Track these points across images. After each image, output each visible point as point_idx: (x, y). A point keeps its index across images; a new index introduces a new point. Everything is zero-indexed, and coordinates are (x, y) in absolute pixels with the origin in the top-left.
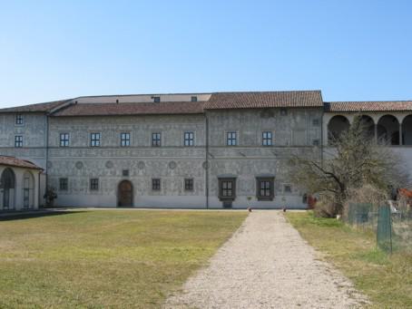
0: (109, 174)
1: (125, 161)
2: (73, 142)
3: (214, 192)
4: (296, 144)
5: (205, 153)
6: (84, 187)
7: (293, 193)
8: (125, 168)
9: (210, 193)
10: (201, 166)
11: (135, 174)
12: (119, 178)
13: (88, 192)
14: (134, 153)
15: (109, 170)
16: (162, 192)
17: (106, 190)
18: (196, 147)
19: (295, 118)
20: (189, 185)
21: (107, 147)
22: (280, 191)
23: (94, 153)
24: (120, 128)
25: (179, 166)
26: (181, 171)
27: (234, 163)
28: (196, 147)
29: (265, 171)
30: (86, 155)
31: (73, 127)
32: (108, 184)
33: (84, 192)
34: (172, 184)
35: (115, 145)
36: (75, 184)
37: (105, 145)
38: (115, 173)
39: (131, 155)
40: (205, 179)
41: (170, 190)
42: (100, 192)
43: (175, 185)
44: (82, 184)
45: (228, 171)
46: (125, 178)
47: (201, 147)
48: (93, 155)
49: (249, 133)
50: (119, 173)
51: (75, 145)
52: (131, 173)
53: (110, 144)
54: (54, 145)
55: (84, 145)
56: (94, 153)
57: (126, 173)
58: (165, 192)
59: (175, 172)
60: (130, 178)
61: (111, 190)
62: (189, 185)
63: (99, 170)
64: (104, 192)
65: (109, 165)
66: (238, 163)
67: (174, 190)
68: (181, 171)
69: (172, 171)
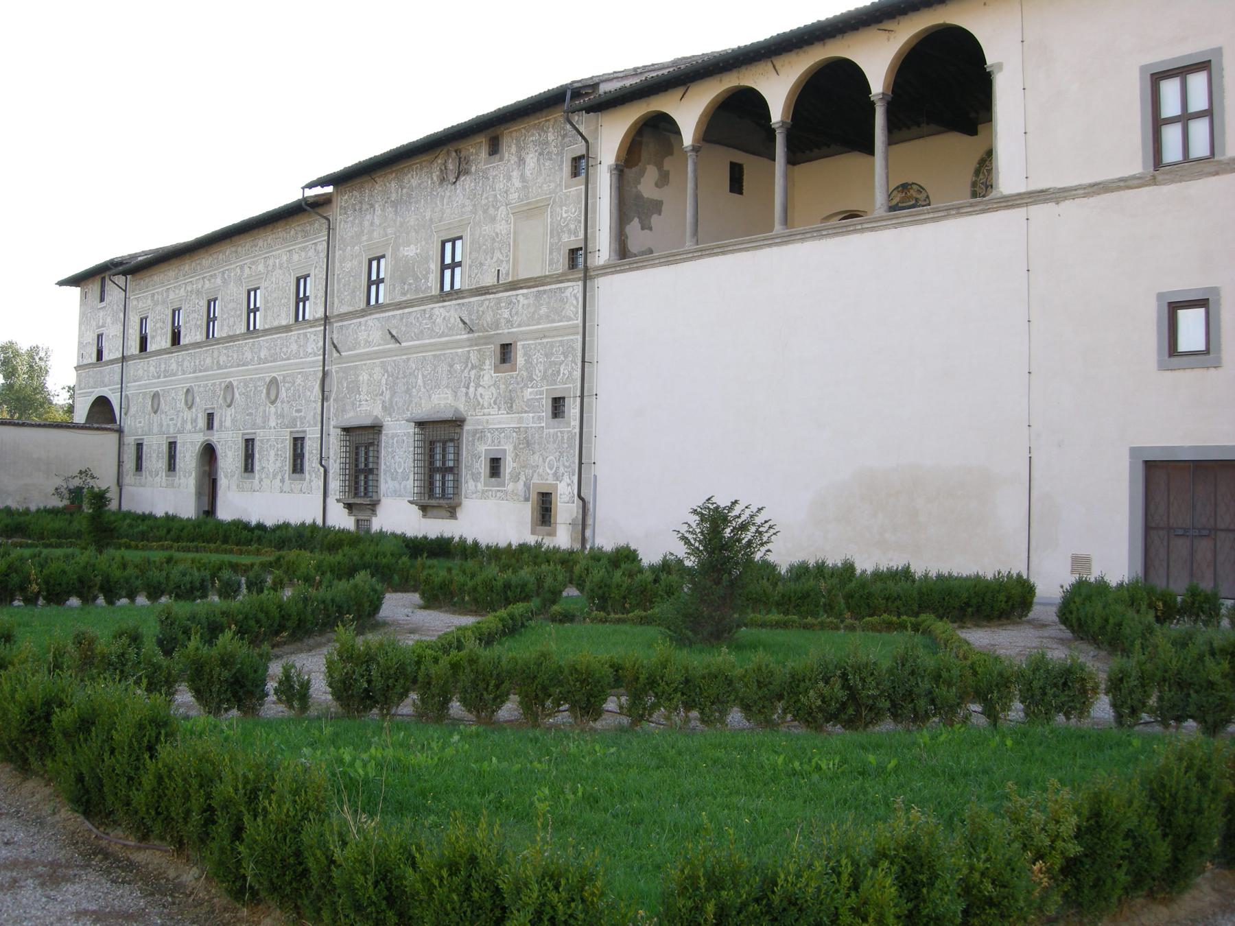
4: (523, 275)
7: (510, 487)
19: (521, 161)
22: (476, 478)
29: (439, 403)
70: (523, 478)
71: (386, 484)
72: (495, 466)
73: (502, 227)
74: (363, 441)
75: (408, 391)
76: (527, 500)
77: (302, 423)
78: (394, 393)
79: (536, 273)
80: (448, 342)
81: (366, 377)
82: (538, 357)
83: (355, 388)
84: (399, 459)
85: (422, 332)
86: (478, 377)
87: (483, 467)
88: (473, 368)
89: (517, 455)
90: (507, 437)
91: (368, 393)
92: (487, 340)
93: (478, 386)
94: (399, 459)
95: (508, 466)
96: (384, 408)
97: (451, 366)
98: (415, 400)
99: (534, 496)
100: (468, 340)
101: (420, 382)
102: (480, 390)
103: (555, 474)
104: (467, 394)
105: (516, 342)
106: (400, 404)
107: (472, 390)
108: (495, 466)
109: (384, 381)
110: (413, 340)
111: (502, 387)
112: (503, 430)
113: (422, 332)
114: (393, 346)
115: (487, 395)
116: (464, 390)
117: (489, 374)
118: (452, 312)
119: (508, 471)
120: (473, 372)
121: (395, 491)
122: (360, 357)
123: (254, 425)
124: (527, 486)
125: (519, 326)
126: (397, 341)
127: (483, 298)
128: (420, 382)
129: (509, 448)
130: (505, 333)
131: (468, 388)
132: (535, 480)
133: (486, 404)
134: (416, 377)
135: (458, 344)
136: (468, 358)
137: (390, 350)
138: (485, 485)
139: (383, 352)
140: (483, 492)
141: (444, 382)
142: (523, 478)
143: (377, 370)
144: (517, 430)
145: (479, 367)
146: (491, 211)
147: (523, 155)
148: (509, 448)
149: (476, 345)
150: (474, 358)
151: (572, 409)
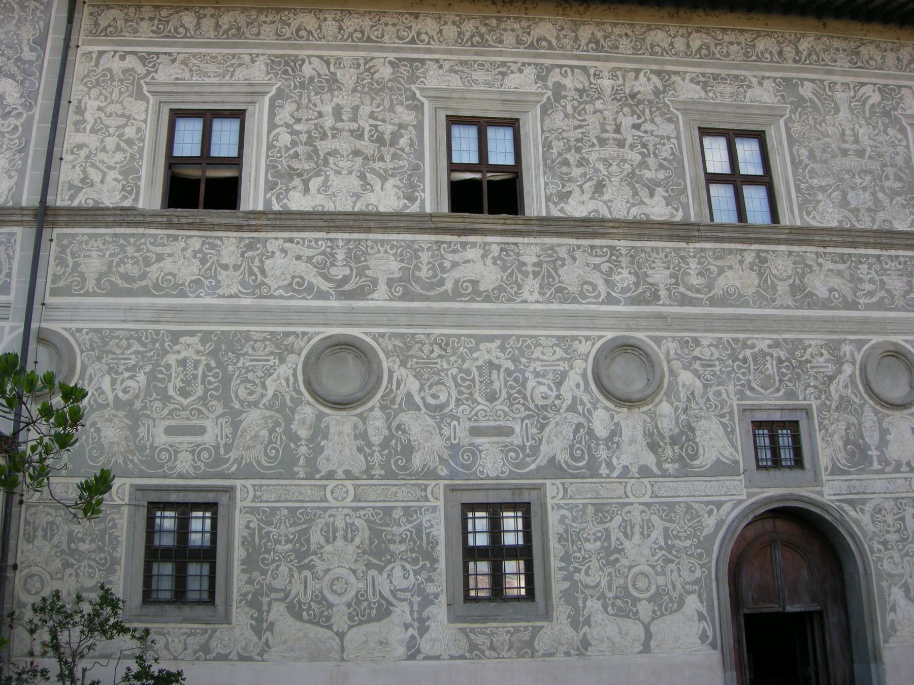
0: (634, 453)
1: (762, 342)
2: (282, 176)
6: (399, 577)
8: (771, 403)
11: (858, 455)
12: (734, 495)
13: (442, 630)
14: (819, 286)
15: (632, 424)
17: (623, 605)
21: (588, 227)
23: (490, 276)
24: (688, 91)
30: (405, 285)
31: (287, 66)
32: (638, 552)
33: (395, 630)
35: (658, 209)
36: (302, 554)
37: (578, 207)
38: (685, 437)
39: (803, 295)
42: (557, 629)
44: (378, 553)
46: (779, 488)
48: (475, 291)
50: (720, 441)
51: (298, 202)
52: (825, 446)
53: (618, 204)
54: (109, 195)
55: (386, 199)
56: (490, 276)
57: (779, 440)
60: (825, 489)
61: (665, 602)
63: (540, 416)
64: (605, 628)
65: (627, 375)
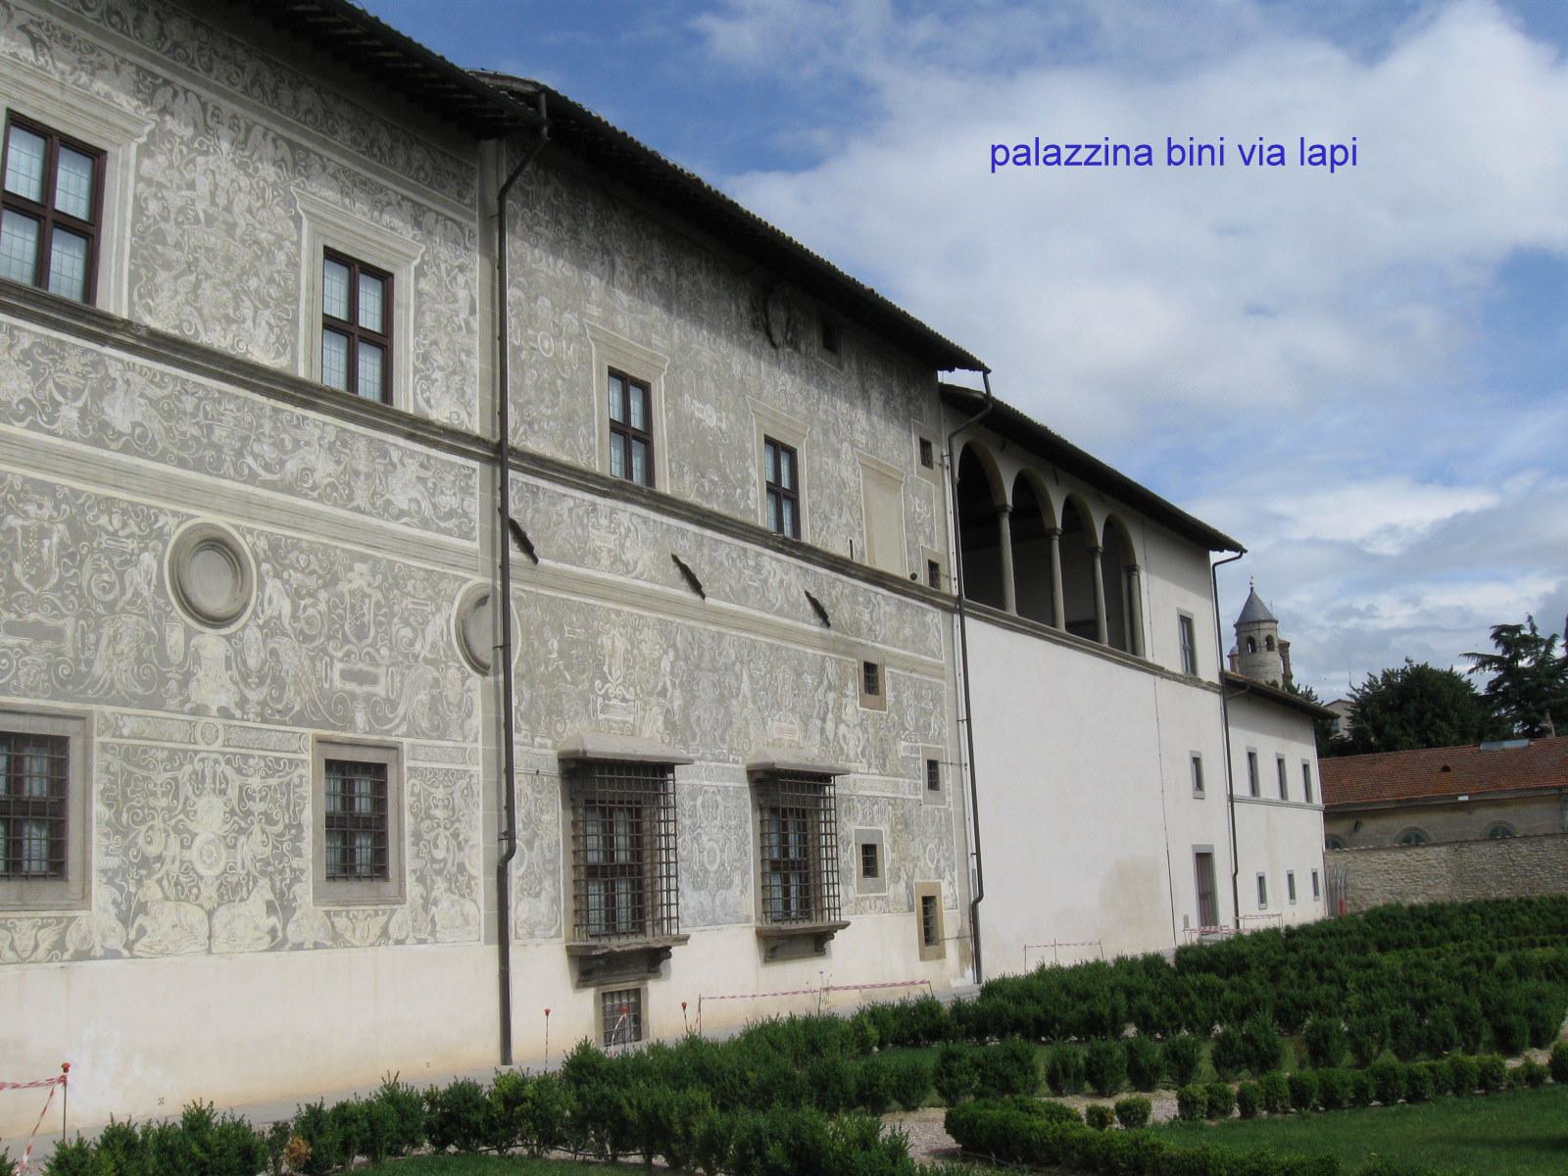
3: (543, 906)
5: (477, 506)
9: (518, 911)
10: (442, 623)
16: (99, 913)
18: (419, 429)
20: (359, 828)
25: (274, 598)
26: (292, 657)
27: (650, 642)
28: (419, 429)
34: (210, 816)
40: (479, 770)
41: (184, 889)
43: (240, 817)
45: (626, 730)
47: (452, 439)
49: (708, 416)
58: (130, 913)
59: (235, 660)
62: (359, 828)
66: (665, 631)
67: (230, 891)
68: (292, 657)
69: (211, 642)
70: (904, 876)
71: (688, 901)
72: (870, 855)
73: (847, 473)
74: (617, 799)
75: (721, 700)
76: (911, 909)
77: (376, 718)
78: (690, 700)
79: (882, 565)
80: (788, 629)
81: (621, 645)
82: (907, 696)
83: (587, 660)
84: (713, 843)
85: (744, 590)
86: (840, 707)
87: (851, 859)
88: (830, 688)
89: (895, 841)
90: (882, 812)
91: (626, 682)
92: (849, 649)
93: (839, 721)
94: (713, 843)
95: (887, 858)
96: (670, 725)
97: (799, 674)
98: (738, 723)
99: (919, 904)
100: (822, 637)
101: (745, 687)
102: (842, 729)
103: (937, 868)
104: (823, 731)
105: (883, 666)
106: (707, 725)
107: (830, 725)
108: (870, 855)
109: (666, 665)
110: (727, 599)
111: (871, 730)
112: (875, 800)
113: (744, 590)
114: (684, 593)
115: (853, 741)
116: (819, 723)
117: (853, 706)
118: (792, 576)
119: (887, 866)
120: (831, 696)
121: (702, 914)
122: (606, 591)
123: (75, 681)
124: (908, 887)
125: (884, 642)
126: (696, 586)
127: (834, 575)
128: (745, 687)
129: (884, 828)
130: (879, 648)
131: (824, 720)
132: (917, 879)
133: (852, 754)
134: (739, 678)
135: (805, 638)
136: (823, 669)
137: (678, 602)
138: (860, 890)
139: (647, 595)
140: (858, 902)
141: (787, 701)
142: (904, 876)
143: (649, 634)
144: (893, 802)
145: (839, 689)
146: (833, 439)
147: (867, 386)
148: (884, 828)
149: (834, 651)
150: (831, 669)
151: (947, 777)
